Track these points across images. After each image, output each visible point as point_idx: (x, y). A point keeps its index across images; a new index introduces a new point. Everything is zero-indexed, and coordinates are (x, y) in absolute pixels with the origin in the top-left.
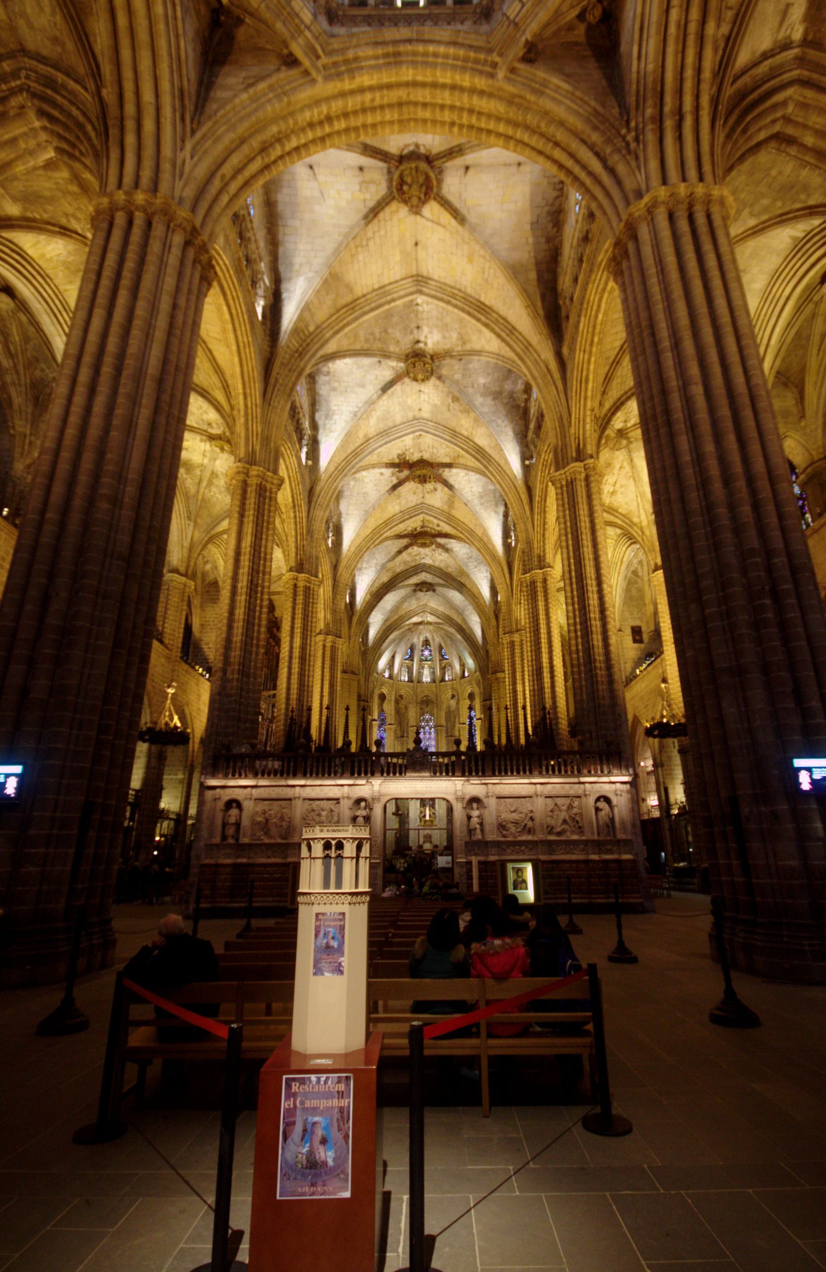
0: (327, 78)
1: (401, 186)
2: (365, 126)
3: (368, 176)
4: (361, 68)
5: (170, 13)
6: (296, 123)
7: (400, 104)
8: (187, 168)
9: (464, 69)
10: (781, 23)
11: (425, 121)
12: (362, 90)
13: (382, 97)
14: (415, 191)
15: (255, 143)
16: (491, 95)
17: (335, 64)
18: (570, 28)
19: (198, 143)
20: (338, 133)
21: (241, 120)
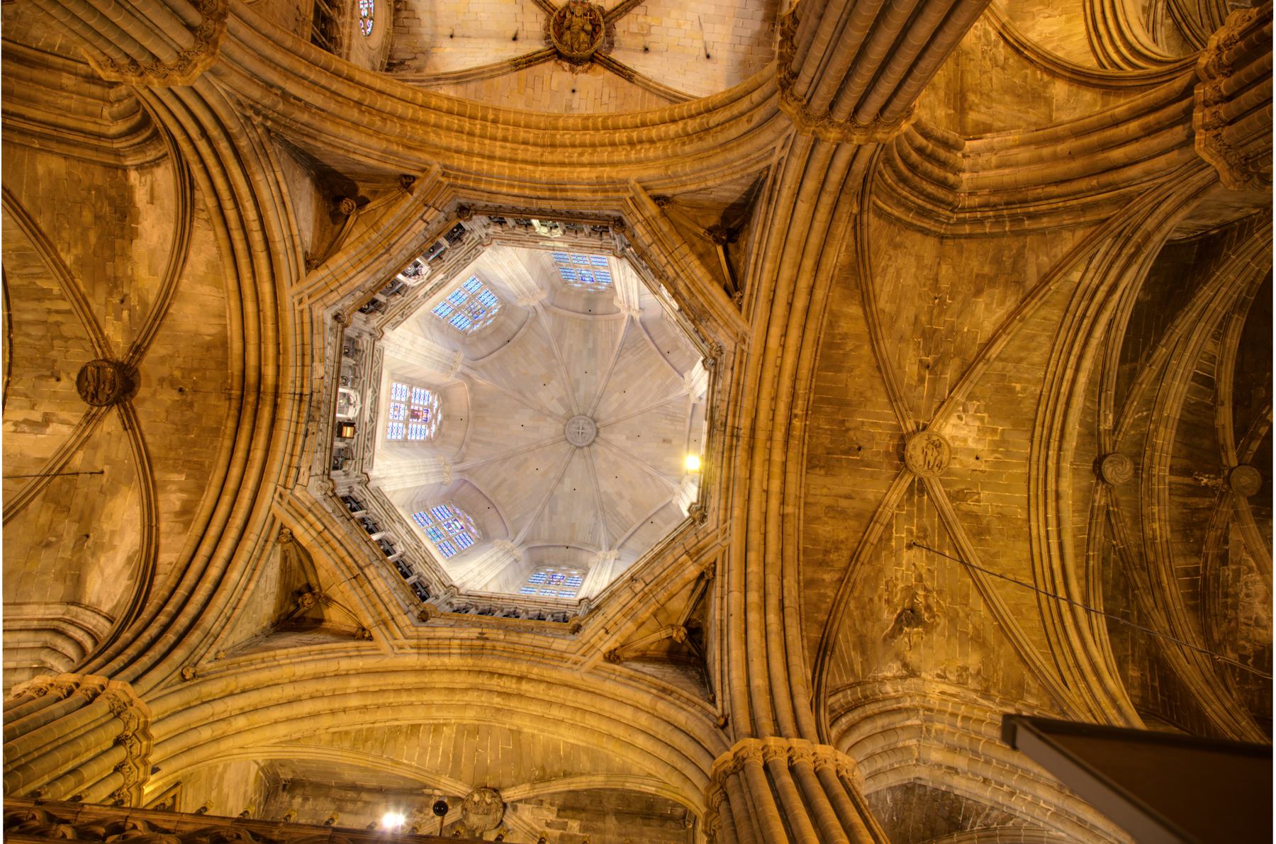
0: (626, 182)
1: (594, 30)
2: (596, 129)
3: (640, 42)
4: (588, 184)
5: (760, 261)
6: (665, 148)
7: (553, 145)
8: (780, 143)
9: (478, 173)
10: (152, 189)
11: (527, 126)
12: (592, 165)
13: (570, 157)
14: (578, 22)
15: (710, 141)
16: (448, 149)
17: (617, 191)
18: (375, 193)
19: (766, 158)
20: (625, 127)
21: (717, 166)
